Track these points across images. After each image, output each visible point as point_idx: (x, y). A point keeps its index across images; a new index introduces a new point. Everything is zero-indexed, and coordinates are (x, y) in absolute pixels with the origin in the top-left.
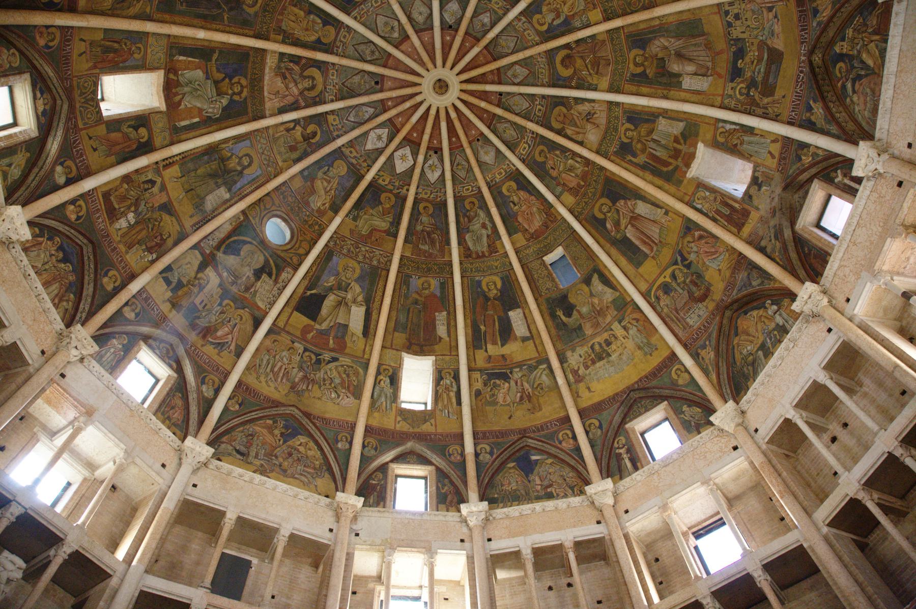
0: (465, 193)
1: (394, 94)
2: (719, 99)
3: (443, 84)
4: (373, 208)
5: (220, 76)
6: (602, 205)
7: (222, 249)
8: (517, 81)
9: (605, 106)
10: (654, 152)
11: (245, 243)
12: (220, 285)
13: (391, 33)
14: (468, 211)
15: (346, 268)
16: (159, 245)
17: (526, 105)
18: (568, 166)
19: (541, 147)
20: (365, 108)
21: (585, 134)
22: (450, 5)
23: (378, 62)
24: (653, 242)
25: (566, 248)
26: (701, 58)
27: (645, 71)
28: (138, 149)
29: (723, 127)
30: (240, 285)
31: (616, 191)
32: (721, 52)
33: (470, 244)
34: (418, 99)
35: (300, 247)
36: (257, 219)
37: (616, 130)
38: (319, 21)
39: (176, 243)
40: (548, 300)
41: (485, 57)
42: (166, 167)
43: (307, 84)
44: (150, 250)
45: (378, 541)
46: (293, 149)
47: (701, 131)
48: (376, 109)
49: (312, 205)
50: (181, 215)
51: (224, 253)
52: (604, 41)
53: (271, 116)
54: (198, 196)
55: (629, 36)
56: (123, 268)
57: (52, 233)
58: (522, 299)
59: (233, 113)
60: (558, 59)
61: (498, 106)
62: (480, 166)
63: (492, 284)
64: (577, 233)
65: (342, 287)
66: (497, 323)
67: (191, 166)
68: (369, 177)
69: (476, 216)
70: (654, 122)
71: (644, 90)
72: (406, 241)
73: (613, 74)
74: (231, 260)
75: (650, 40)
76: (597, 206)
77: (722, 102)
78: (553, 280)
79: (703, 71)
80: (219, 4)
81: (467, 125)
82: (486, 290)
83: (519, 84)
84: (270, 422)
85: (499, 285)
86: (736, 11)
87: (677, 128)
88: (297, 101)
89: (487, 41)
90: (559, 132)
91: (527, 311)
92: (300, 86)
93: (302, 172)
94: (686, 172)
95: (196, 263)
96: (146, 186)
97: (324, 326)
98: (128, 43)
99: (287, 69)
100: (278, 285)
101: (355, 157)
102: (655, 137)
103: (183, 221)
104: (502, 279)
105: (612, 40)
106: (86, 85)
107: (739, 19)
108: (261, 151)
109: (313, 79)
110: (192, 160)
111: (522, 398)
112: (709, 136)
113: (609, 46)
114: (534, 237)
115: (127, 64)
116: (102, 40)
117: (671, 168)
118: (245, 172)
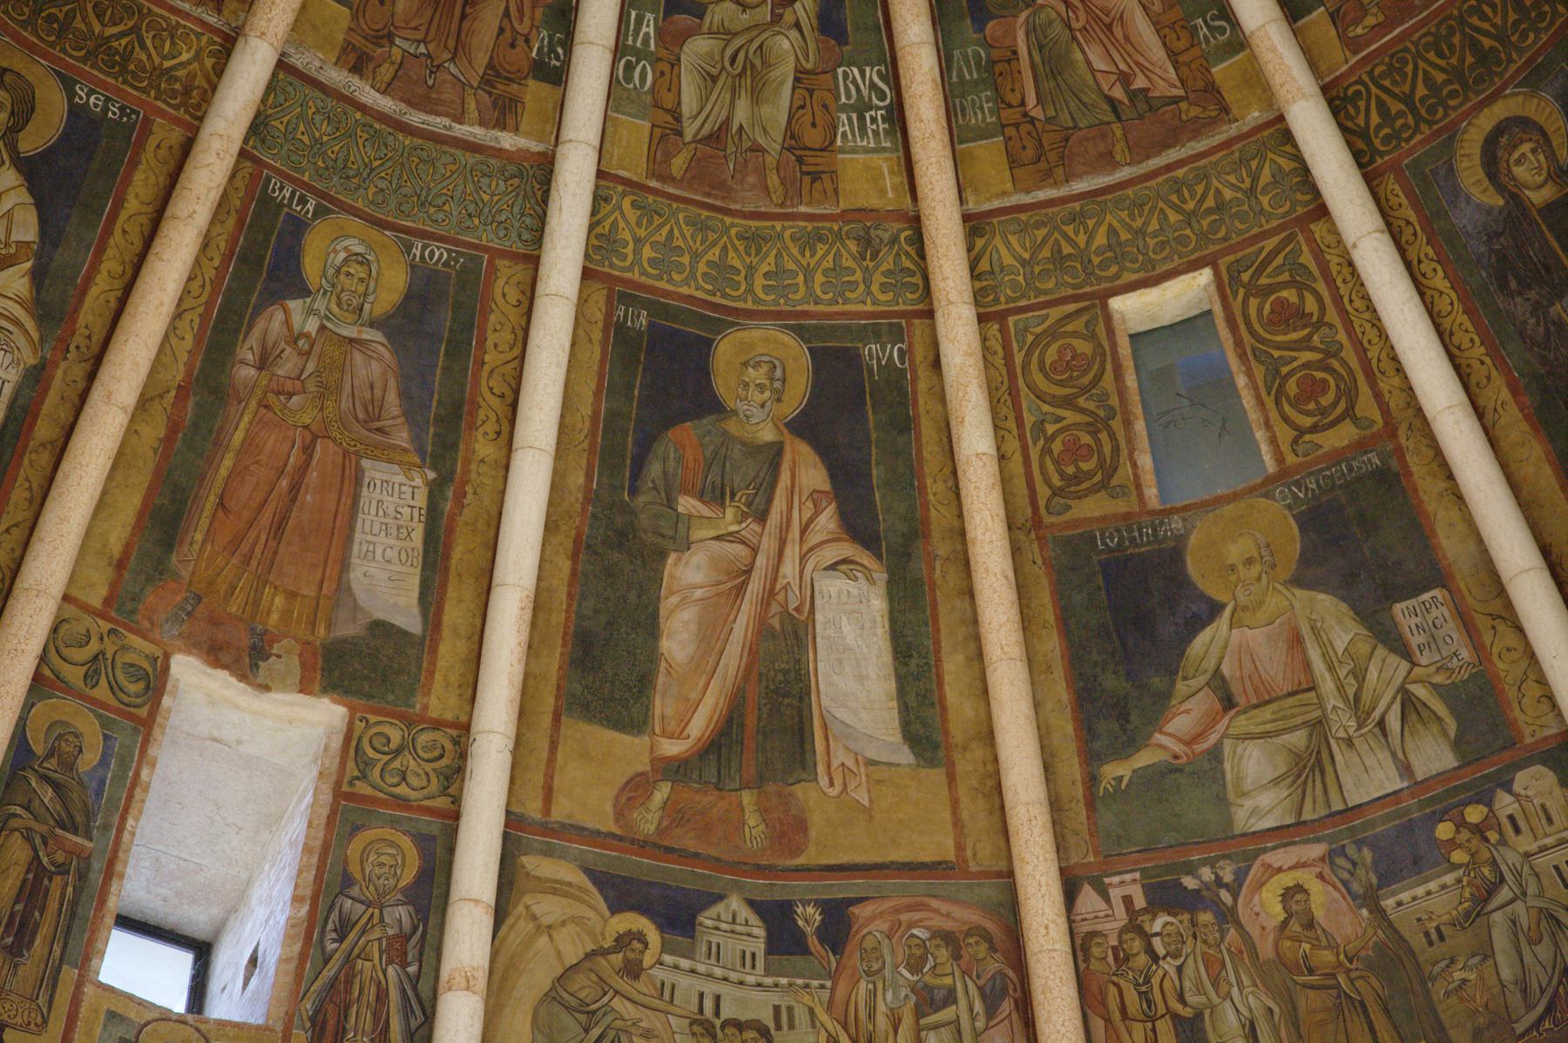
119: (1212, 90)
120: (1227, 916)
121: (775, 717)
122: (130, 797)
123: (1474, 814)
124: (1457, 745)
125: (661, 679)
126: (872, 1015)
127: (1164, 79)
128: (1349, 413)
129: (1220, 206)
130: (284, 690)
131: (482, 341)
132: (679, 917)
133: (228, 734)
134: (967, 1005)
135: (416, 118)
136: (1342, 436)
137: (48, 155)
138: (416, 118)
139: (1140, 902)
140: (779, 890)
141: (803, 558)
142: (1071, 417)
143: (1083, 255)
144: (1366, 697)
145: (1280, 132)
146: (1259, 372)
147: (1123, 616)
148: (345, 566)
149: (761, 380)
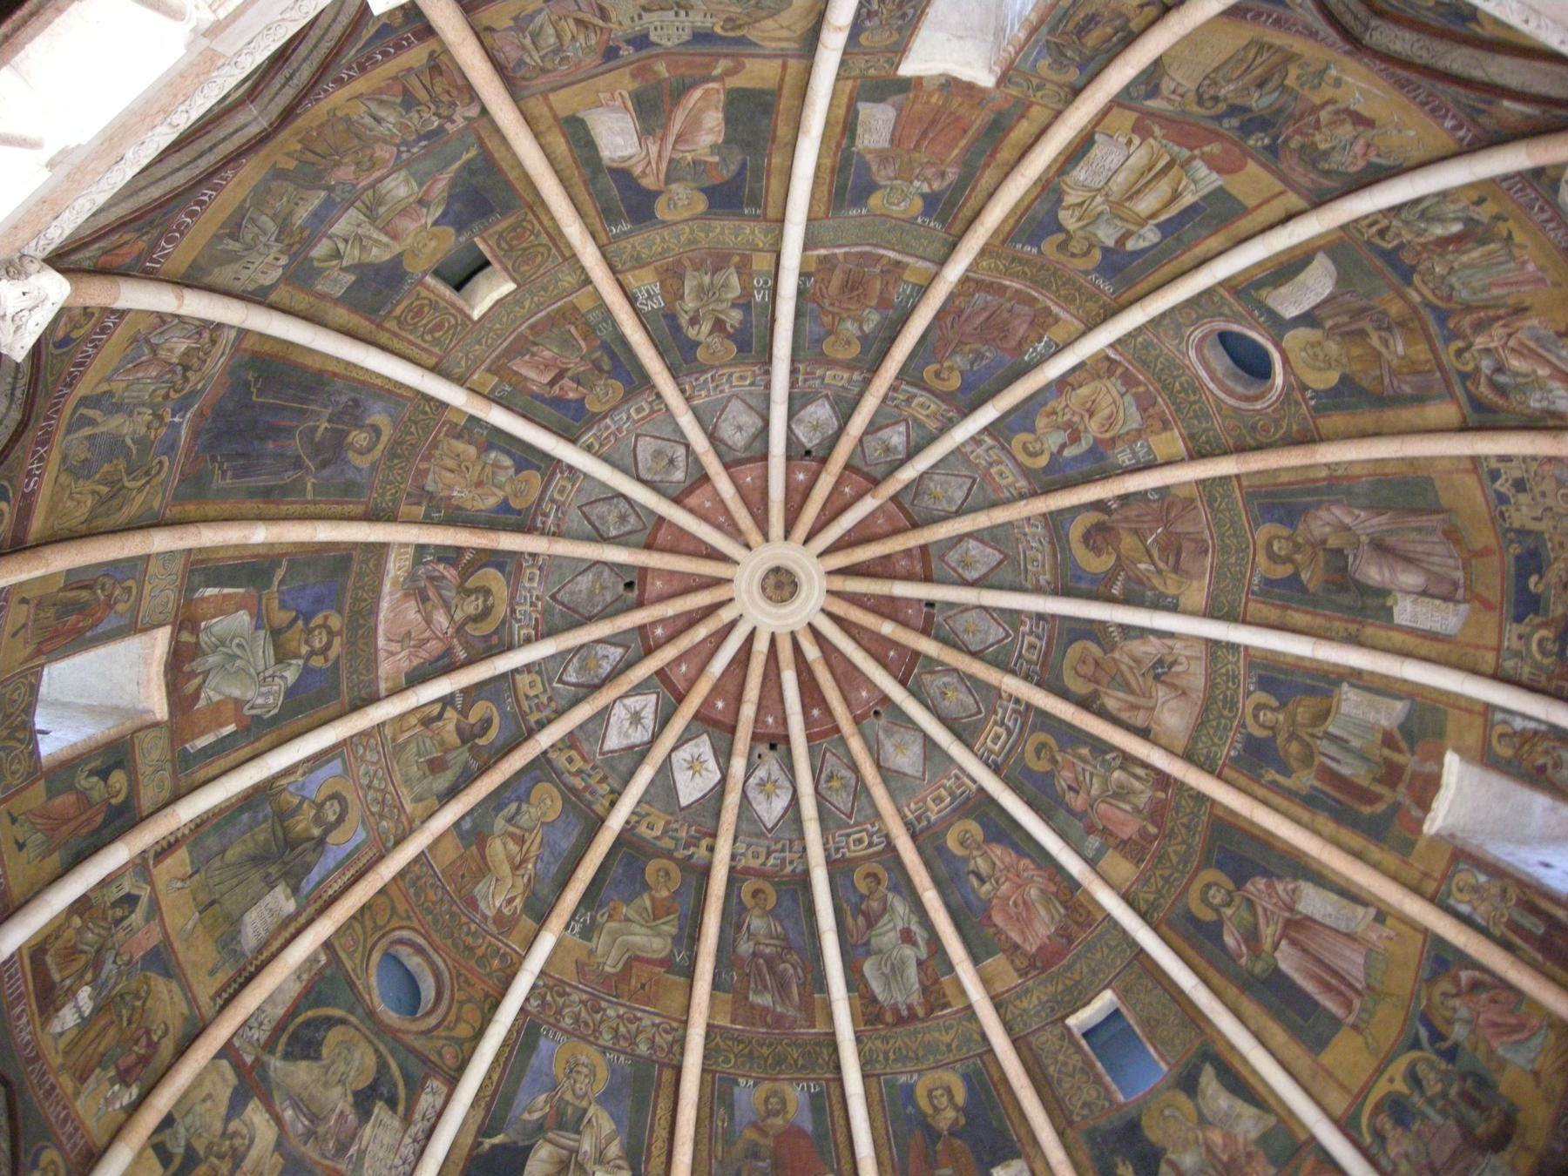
0: (855, 851)
2: (1490, 657)
3: (784, 578)
4: (628, 901)
5: (281, 617)
6: (1208, 886)
7: (281, 1047)
9: (1199, 651)
10: (1334, 765)
11: (331, 1022)
12: (279, 1146)
13: (667, 473)
14: (863, 897)
15: (572, 1069)
16: (144, 1060)
17: (995, 633)
18: (1113, 787)
19: (1041, 736)
20: (601, 650)
21: (1153, 709)
22: (811, 409)
23: (633, 538)
24: (1350, 986)
25: (1124, 993)
26: (1436, 559)
27: (1295, 576)
28: (105, 824)
29: (1505, 722)
30: (325, 1141)
31: (1243, 855)
32: (1485, 552)
33: (877, 987)
35: (458, 1019)
36: (358, 955)
37: (1232, 704)
38: (508, 462)
39: (182, 1051)
40: (1090, 1135)
41: (890, 518)
43: (472, 606)
44: (124, 1078)
46: (436, 766)
47: (1451, 726)
48: (627, 648)
49: (482, 905)
50: (189, 973)
51: (287, 1056)
52: (1192, 500)
53: (392, 693)
54: (228, 917)
55: (1250, 496)
56: (71, 1136)
58: (1022, 1132)
59: (309, 704)
60: (1076, 530)
61: (925, 631)
62: (886, 781)
63: (941, 1092)
64: (1148, 956)
65: (567, 1120)
67: (213, 842)
68: (616, 822)
69: (884, 910)
70: (1328, 694)
71: (1299, 618)
72: (716, 985)
73: (1218, 573)
74: (302, 1073)
75: (1305, 510)
76: (1197, 886)
77: (1498, 666)
78: (1098, 1080)
79: (1444, 588)
80: (299, 457)
81: (847, 675)
82: (930, 1111)
85: (960, 1096)
86: (1517, 474)
87: (1391, 713)
88: (449, 651)
89: (899, 486)
90: (1084, 704)
91: (1038, 1166)
92: (459, 616)
93: (457, 824)
94: (1421, 822)
95: (224, 1094)
96: (119, 913)
98: (109, 583)
99: (431, 579)
100: (413, 1130)
101: (580, 772)
102: (1332, 730)
103: (195, 987)
104: (966, 1077)
105: (1211, 500)
106: (15, 697)
107: (1524, 490)
108: (365, 781)
109: (487, 592)
110: (217, 828)
112: (1472, 738)
113: (1203, 514)
114: (1038, 964)
115: (100, 630)
116: (60, 590)
117: (1380, 807)
118: (331, 839)
119: (495, 373)
122: (1021, 49)
123: (295, 248)
124: (312, 259)
125: (721, 105)
126: (587, 37)
127: (522, 367)
128: (398, 319)
129: (479, 342)
130: (932, 77)
131: (830, 191)
132: (702, 37)
133: (955, 44)
135: (867, 249)
136: (398, 311)
137: (1052, 233)
138: (867, 249)
139: (448, 126)
140: (644, 53)
141: (648, 154)
142: (525, 245)
143: (532, 294)
144: (357, 244)
145: (460, 381)
146: (443, 304)
148: (898, 116)
149: (682, 203)
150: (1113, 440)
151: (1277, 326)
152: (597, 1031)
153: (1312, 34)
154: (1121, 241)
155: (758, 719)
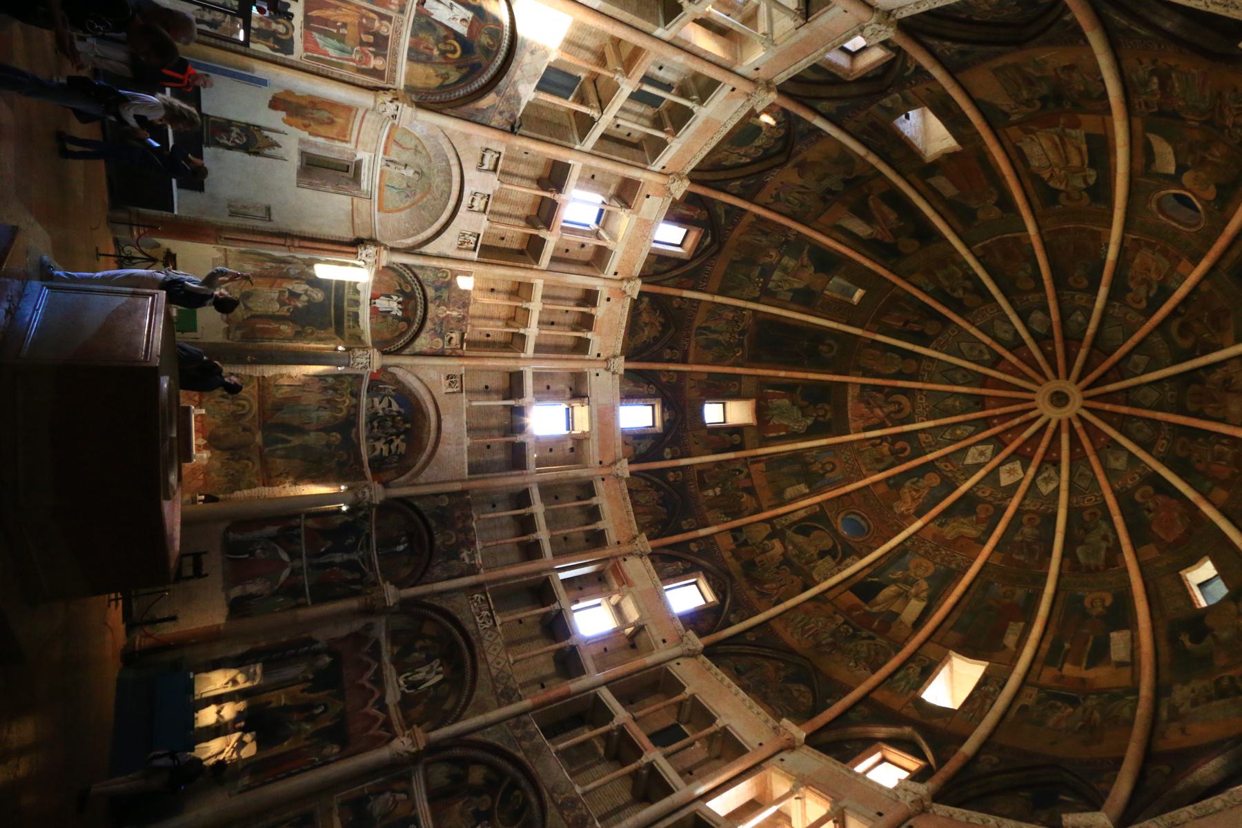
0: (1087, 504)
1: (998, 412)
8: (1141, 370)
11: (817, 528)
12: (783, 554)
15: (918, 566)
33: (1081, 557)
34: (1032, 414)
42: (753, 463)
43: (892, 408)
44: (727, 515)
45: (795, 772)
46: (878, 461)
53: (857, 432)
57: (659, 488)
61: (1127, 405)
63: (1098, 600)
66: (1090, 643)
72: (997, 548)
74: (800, 539)
83: (1143, 373)
84: (782, 665)
85: (1108, 603)
95: (765, 534)
97: (875, 609)
109: (900, 404)
111: (1082, 727)
118: (828, 475)
120: (776, 247)
121: (863, 213)
132: (847, 182)
134: (797, 209)
145: (861, 327)
147: (826, 262)
149: (908, 245)
150: (1164, 279)
151: (1175, 179)
152: (935, 557)
153: (1000, 54)
154: (1085, 181)
155: (1047, 453)
